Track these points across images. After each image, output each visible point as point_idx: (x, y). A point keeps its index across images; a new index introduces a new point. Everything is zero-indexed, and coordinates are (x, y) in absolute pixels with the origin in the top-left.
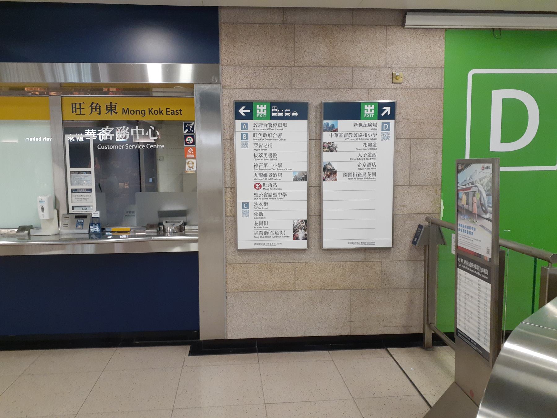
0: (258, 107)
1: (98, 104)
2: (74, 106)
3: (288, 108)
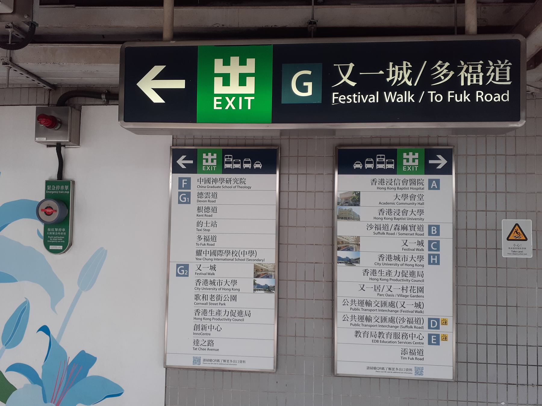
0: (204, 156)
3: (247, 157)
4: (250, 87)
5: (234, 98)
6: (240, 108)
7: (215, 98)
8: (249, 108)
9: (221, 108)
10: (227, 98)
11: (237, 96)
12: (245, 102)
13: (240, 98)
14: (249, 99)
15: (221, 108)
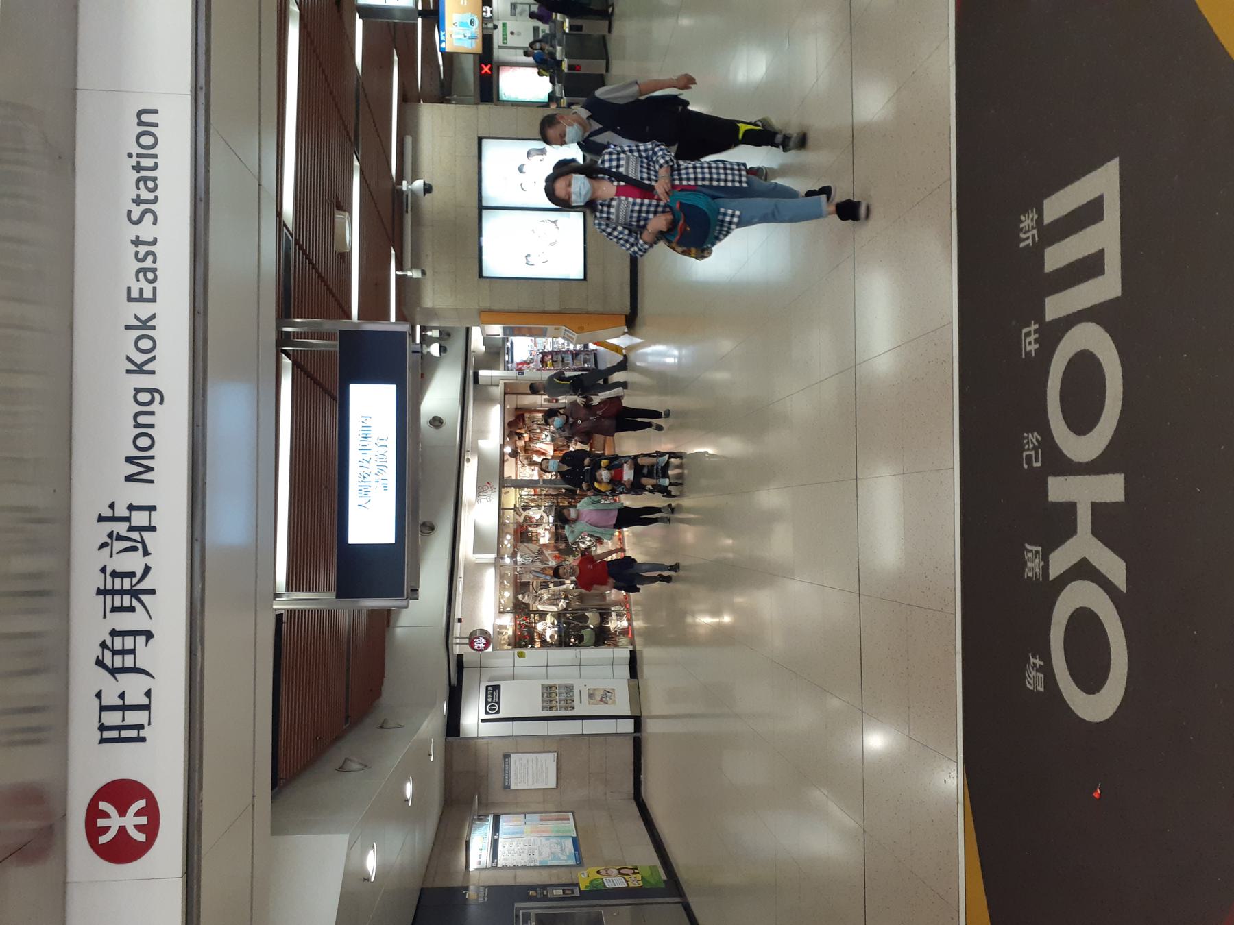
1: (103, 645)
2: (114, 734)
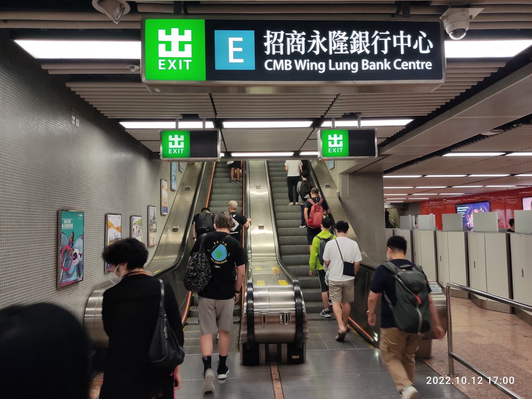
4: (188, 52)
5: (175, 61)
6: (181, 68)
7: (160, 61)
8: (188, 68)
9: (164, 69)
10: (170, 61)
11: (178, 59)
12: (184, 64)
13: (180, 61)
14: (188, 61)
15: (164, 69)
